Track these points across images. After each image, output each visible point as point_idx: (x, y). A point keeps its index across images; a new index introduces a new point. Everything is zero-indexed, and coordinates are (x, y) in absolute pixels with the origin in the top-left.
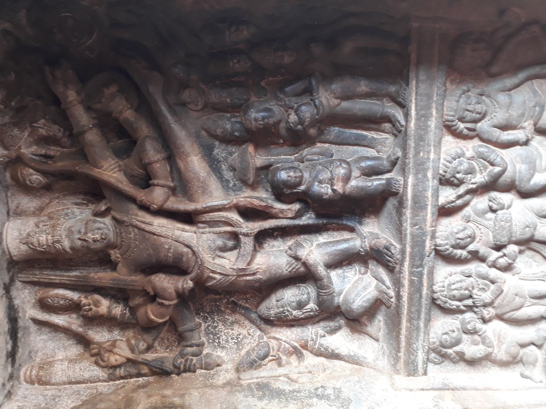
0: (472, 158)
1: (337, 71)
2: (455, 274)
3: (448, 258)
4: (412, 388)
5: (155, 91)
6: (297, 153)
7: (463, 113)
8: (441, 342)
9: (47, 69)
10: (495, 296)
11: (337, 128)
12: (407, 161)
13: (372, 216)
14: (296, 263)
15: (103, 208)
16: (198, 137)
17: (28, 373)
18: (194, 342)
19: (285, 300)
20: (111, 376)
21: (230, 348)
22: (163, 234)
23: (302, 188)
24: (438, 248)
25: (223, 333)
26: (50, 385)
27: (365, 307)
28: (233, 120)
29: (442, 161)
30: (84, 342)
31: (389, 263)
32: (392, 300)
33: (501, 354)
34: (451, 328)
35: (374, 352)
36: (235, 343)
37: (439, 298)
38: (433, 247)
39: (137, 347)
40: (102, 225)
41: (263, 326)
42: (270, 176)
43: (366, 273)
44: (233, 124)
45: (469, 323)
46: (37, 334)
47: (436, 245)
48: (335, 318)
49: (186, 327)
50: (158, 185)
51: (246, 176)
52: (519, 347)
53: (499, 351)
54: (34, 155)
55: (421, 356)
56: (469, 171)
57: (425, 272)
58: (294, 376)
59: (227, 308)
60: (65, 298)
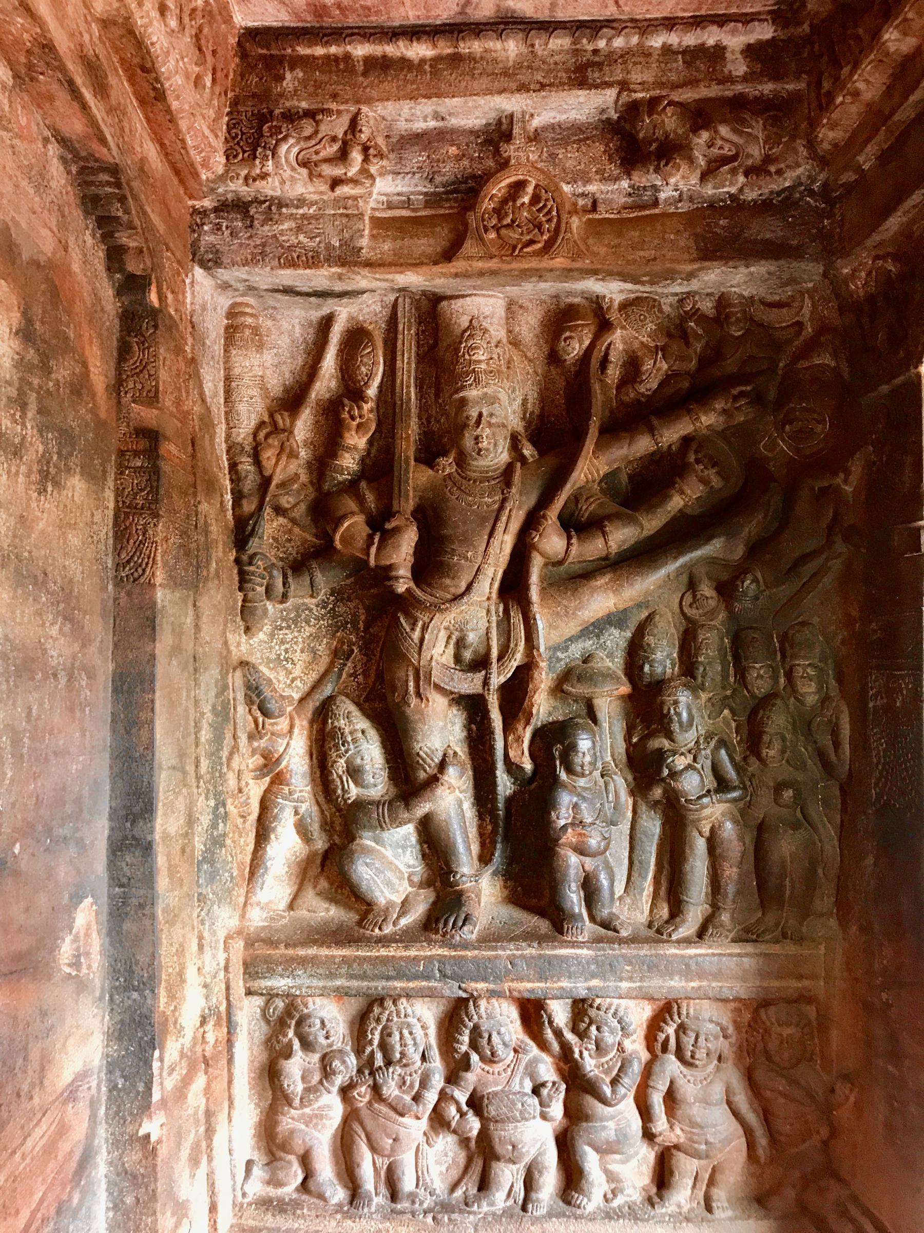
0: (621, 1049)
2: (426, 1034)
4: (231, 970)
6: (616, 766)
7: (692, 1030)
8: (309, 1016)
10: (393, 1104)
11: (658, 831)
12: (616, 946)
13: (506, 892)
14: (433, 764)
15: (526, 452)
17: (248, 310)
18: (292, 588)
20: (239, 448)
21: (271, 648)
22: (491, 550)
23: (563, 776)
24: (471, 1003)
25: (296, 634)
28: (668, 662)
30: (292, 400)
31: (442, 921)
32: (377, 930)
33: (289, 1121)
34: (332, 1032)
36: (279, 655)
37: (384, 1009)
38: (475, 994)
39: (287, 494)
40: (500, 450)
45: (344, 1062)
47: (475, 1000)
48: (325, 830)
49: (319, 575)
50: (569, 544)
51: (579, 680)
52: (302, 1152)
53: (293, 1119)
54: (610, 345)
55: (281, 983)
56: (602, 1045)
57: (433, 984)
58: (235, 763)
59: (341, 642)
60: (370, 376)
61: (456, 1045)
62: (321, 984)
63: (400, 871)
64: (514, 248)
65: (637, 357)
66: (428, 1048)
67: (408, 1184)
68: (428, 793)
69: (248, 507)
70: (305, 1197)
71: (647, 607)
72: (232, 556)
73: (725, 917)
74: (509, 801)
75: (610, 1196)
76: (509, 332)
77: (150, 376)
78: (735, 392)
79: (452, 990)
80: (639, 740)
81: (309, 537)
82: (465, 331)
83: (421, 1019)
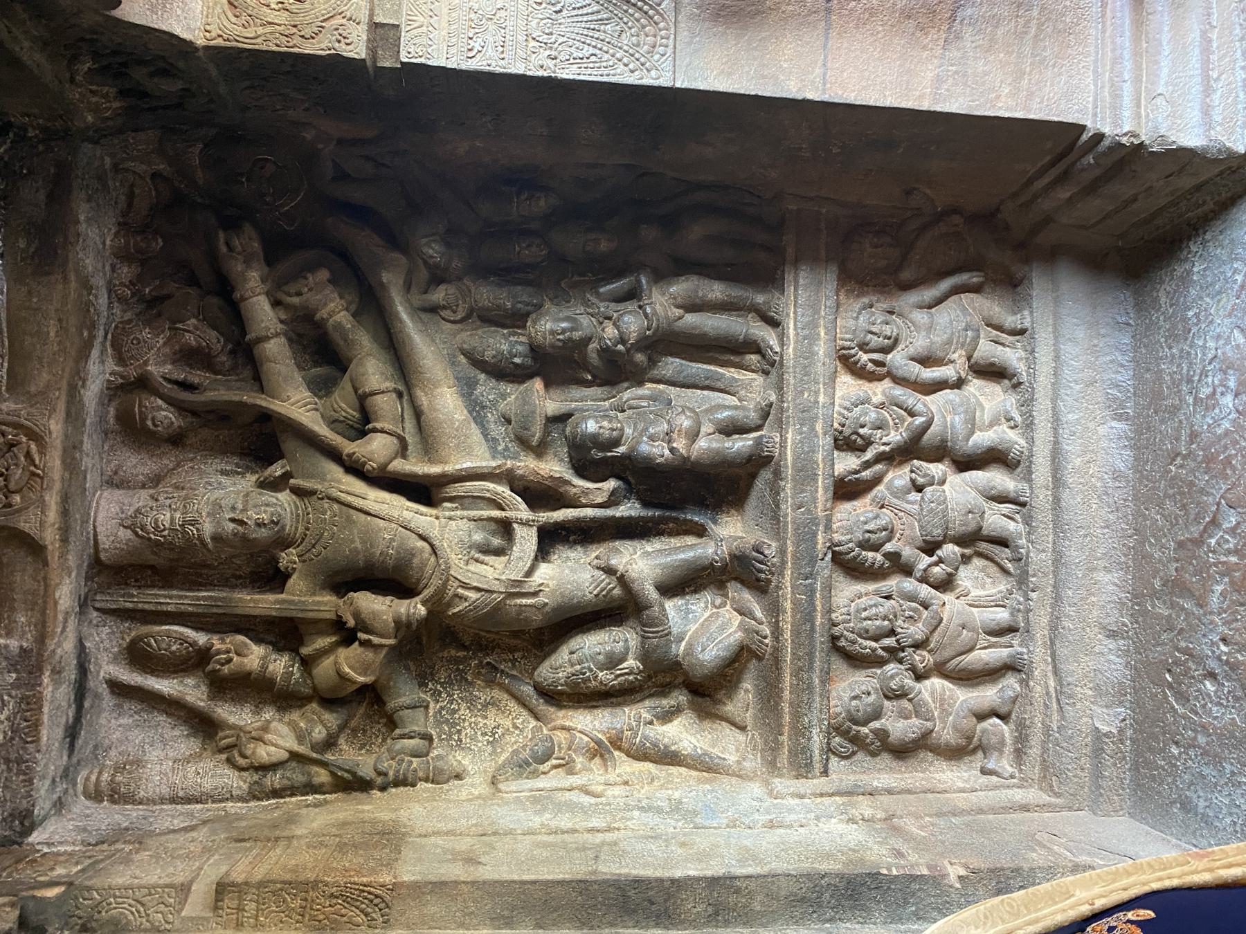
0: (882, 406)
1: (681, 266)
3: (854, 570)
4: (802, 792)
5: (392, 281)
8: (849, 711)
9: (221, 235)
13: (733, 511)
16: (453, 363)
17: (93, 778)
19: (586, 651)
20: (256, 787)
21: (479, 751)
22: (382, 514)
23: (622, 449)
26: (134, 802)
27: (723, 659)
29: (837, 408)
30: (203, 726)
32: (767, 641)
33: (946, 734)
34: (864, 688)
35: (737, 750)
36: (488, 742)
37: (842, 635)
41: (543, 707)
42: (568, 429)
43: (723, 605)
44: (512, 345)
45: (892, 677)
46: (115, 715)
48: (669, 692)
49: (403, 699)
50: (382, 431)
54: (165, 379)
55: (817, 739)
58: (600, 788)
60: (183, 640)
61: (877, 565)
62: (818, 699)
63: (710, 616)
64: (34, 474)
65: (181, 351)
66: (877, 593)
67: (1002, 615)
68: (636, 586)
69: (322, 776)
70: (1013, 716)
71: (455, 356)
72: (376, 793)
73: (760, 299)
74: (646, 504)
75: (1012, 423)
76: (143, 487)
77: (150, 894)
78: (224, 249)
79: (825, 566)
80: (590, 372)
81: (361, 711)
82: (136, 534)
83: (852, 600)
